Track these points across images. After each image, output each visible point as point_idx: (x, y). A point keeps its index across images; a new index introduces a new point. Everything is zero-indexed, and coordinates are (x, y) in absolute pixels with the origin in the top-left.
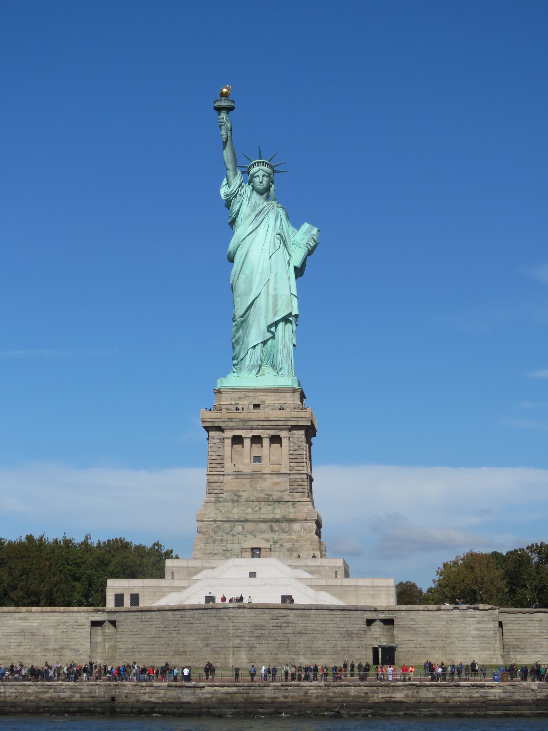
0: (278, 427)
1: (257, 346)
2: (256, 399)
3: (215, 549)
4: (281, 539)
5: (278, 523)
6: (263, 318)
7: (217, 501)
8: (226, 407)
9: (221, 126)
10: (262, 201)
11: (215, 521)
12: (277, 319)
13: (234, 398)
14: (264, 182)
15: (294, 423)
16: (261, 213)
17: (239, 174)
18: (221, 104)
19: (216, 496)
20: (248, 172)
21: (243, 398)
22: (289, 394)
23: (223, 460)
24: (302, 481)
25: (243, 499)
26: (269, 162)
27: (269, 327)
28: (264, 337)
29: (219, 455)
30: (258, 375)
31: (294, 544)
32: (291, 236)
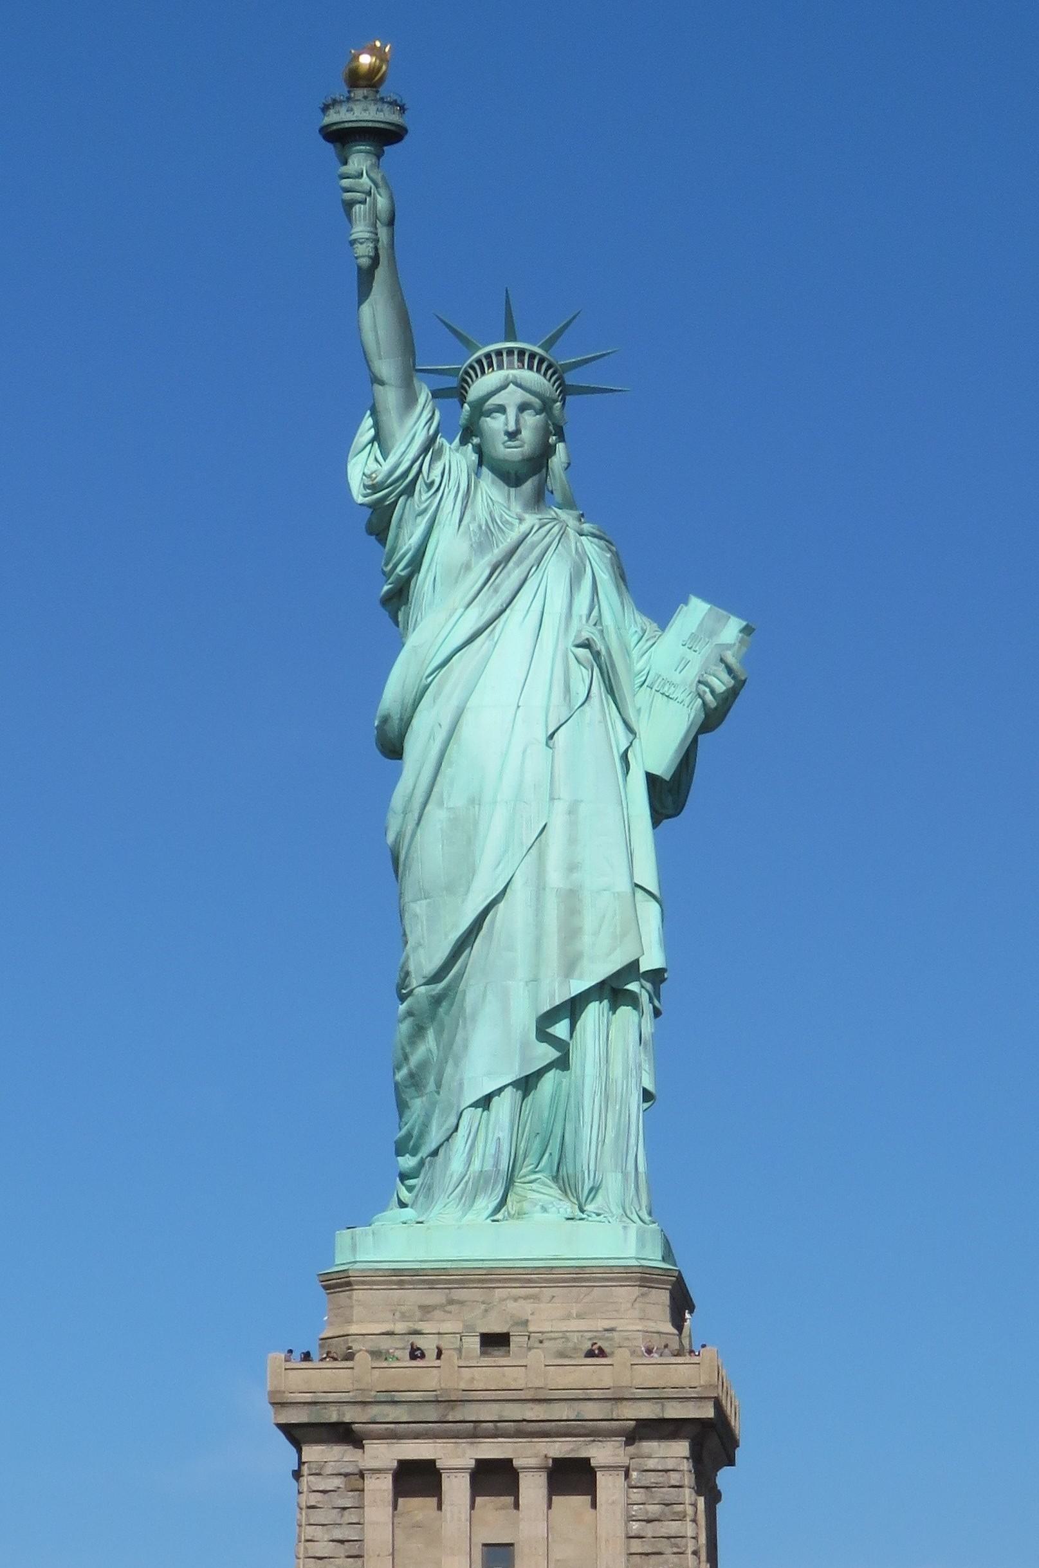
0: (584, 1427)
6: (522, 984)
8: (370, 1343)
9: (349, 205)
10: (517, 508)
12: (578, 986)
13: (404, 1308)
14: (526, 435)
15: (647, 1411)
16: (515, 558)
17: (422, 399)
18: (350, 116)
20: (460, 393)
21: (441, 1307)
22: (626, 1294)
26: (547, 351)
27: (547, 1019)
28: (524, 1059)
29: (342, 1542)
30: (499, 1216)
32: (635, 653)
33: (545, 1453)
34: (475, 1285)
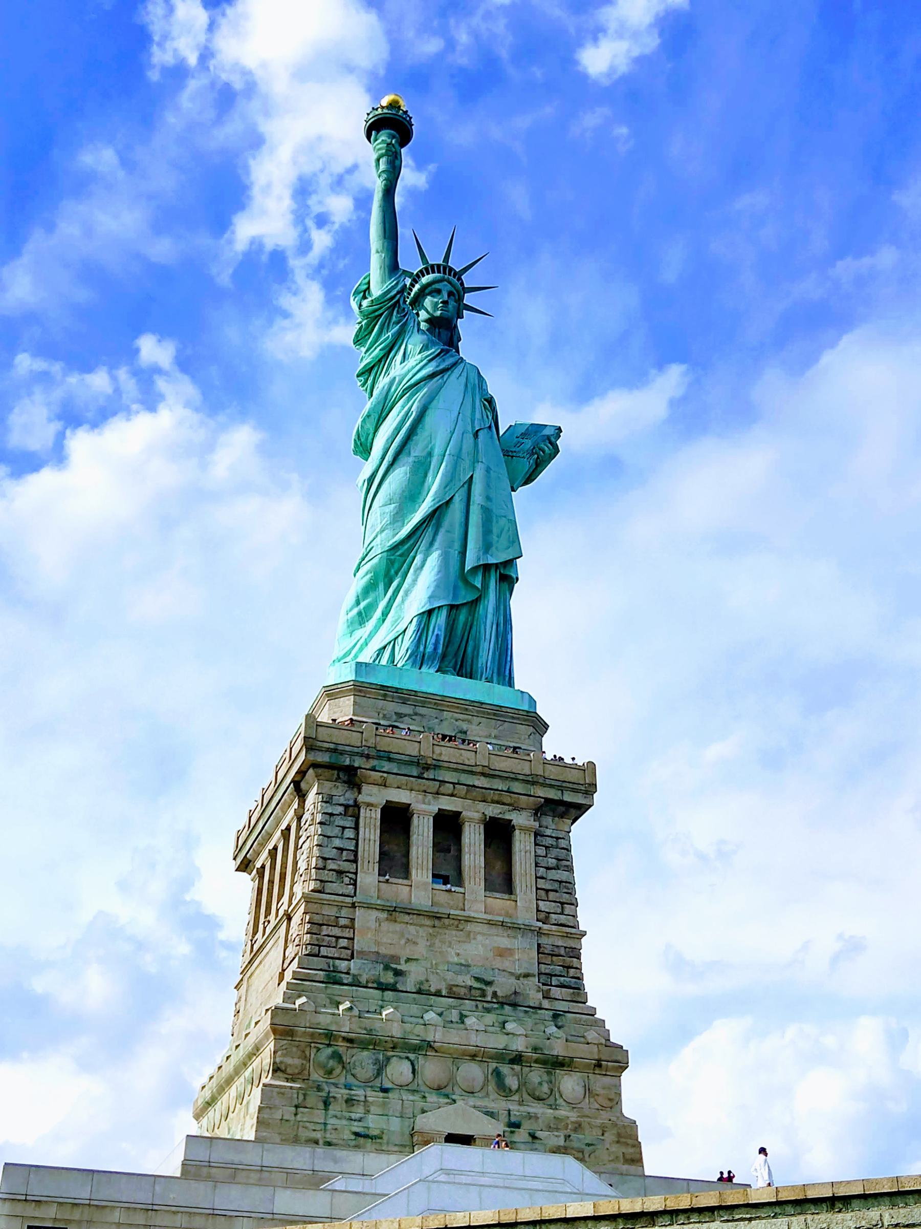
1: (436, 611)
2: (445, 723)
3: (329, 1127)
4: (530, 1116)
5: (517, 1068)
6: (457, 552)
7: (333, 978)
11: (330, 1036)
15: (553, 794)
19: (328, 965)
21: (409, 715)
23: (355, 865)
24: (571, 954)
25: (409, 984)
28: (455, 596)
31: (569, 1136)
33: (483, 811)
34: (432, 706)
